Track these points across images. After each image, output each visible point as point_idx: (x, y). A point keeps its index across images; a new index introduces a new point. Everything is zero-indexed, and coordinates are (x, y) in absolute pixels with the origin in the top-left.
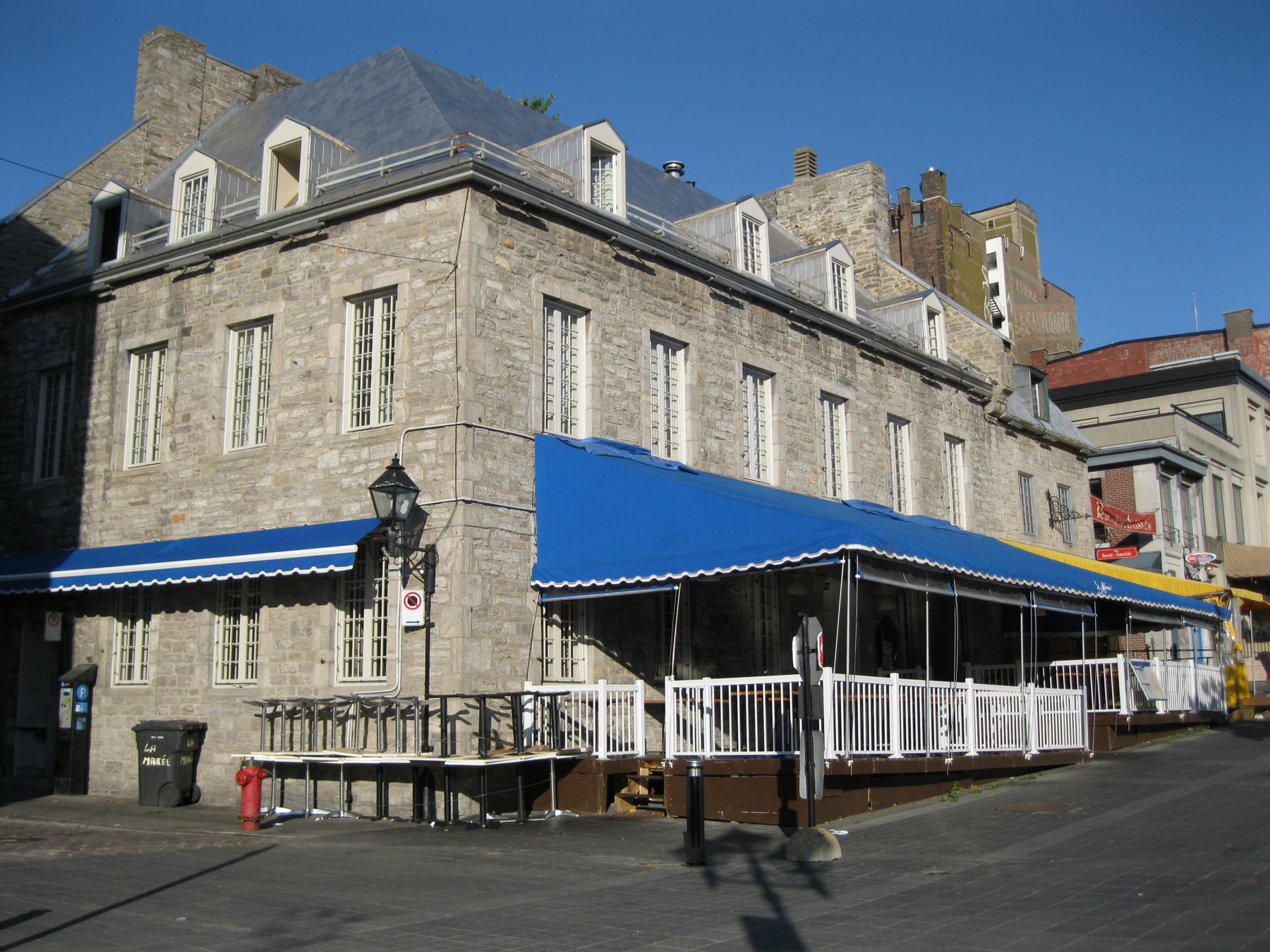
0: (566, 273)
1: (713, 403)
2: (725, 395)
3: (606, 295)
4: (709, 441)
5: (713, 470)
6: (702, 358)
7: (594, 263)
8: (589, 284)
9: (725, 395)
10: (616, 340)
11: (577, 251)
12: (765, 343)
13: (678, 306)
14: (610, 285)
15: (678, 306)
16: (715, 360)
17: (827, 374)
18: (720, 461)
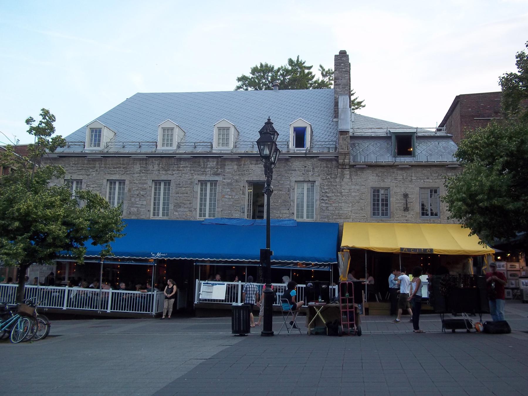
0: (74, 171)
1: (136, 196)
2: (142, 193)
3: (88, 173)
4: (132, 209)
5: (133, 217)
6: (131, 183)
7: (85, 166)
8: (83, 172)
9: (142, 193)
10: (92, 186)
11: (78, 164)
12: (166, 171)
13: (122, 169)
14: (91, 170)
15: (122, 169)
16: (137, 182)
17: (204, 173)
18: (139, 213)
